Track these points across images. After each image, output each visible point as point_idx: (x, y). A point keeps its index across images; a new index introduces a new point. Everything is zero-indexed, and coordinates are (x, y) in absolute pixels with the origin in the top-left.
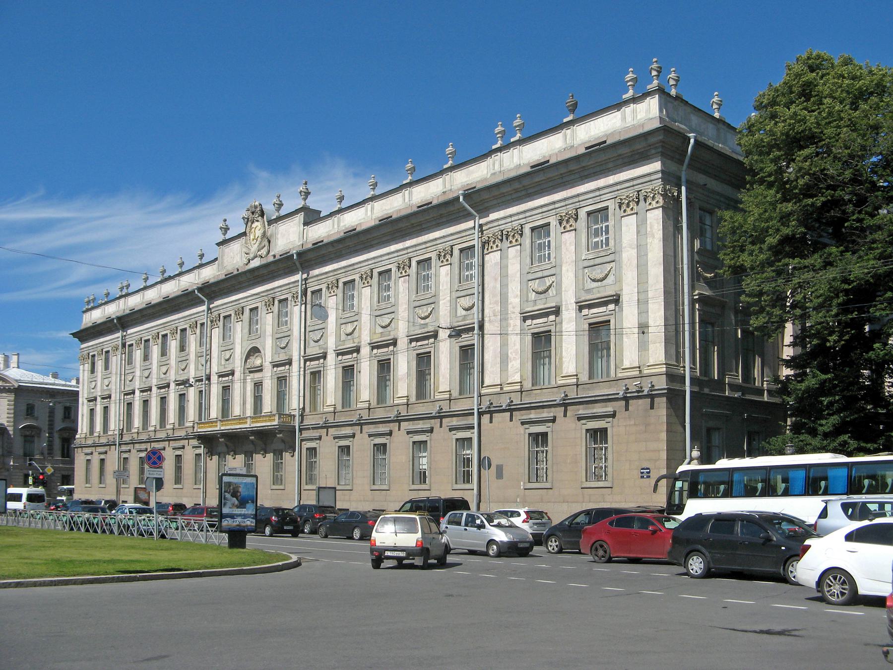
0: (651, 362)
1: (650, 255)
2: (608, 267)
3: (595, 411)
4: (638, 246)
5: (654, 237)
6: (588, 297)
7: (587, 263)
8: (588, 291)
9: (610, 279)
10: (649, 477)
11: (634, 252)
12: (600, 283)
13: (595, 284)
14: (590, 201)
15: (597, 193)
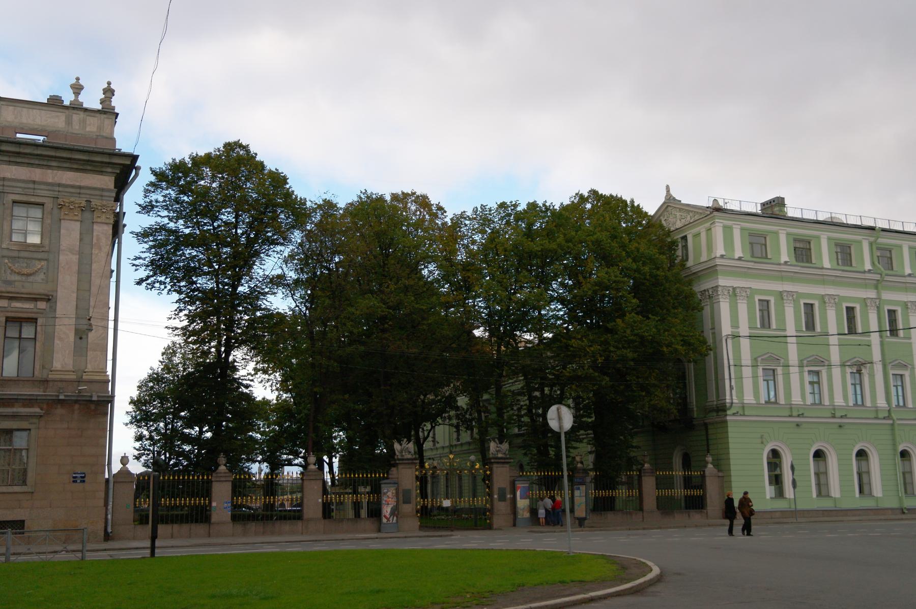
0: (89, 368)
1: (94, 266)
2: (38, 265)
3: (15, 410)
4: (81, 253)
5: (100, 249)
6: (10, 289)
7: (6, 253)
8: (9, 283)
9: (40, 277)
10: (84, 481)
11: (75, 258)
12: (24, 278)
13: (17, 278)
14: (19, 190)
15: (31, 186)
